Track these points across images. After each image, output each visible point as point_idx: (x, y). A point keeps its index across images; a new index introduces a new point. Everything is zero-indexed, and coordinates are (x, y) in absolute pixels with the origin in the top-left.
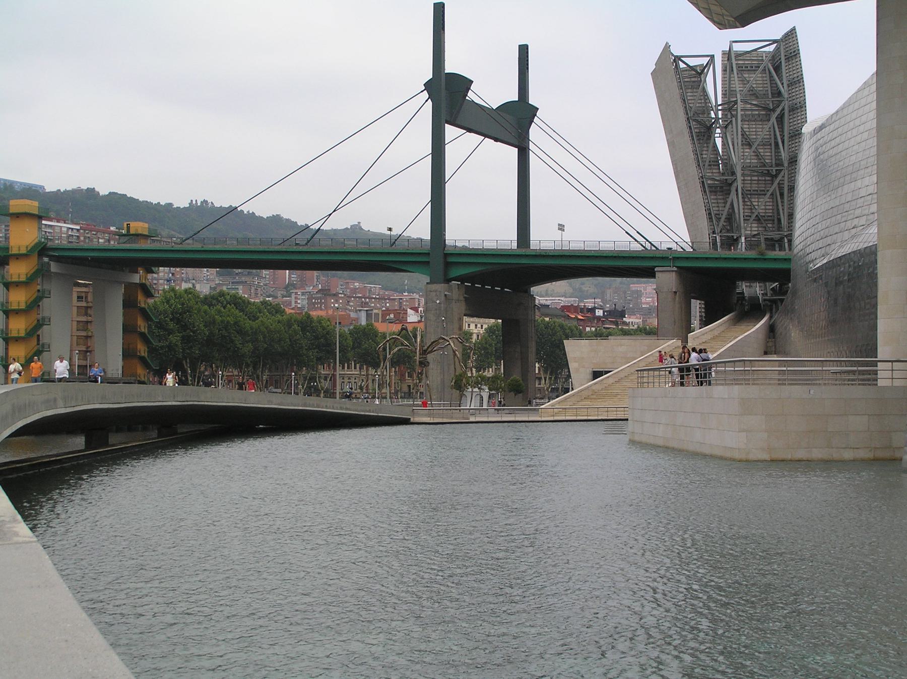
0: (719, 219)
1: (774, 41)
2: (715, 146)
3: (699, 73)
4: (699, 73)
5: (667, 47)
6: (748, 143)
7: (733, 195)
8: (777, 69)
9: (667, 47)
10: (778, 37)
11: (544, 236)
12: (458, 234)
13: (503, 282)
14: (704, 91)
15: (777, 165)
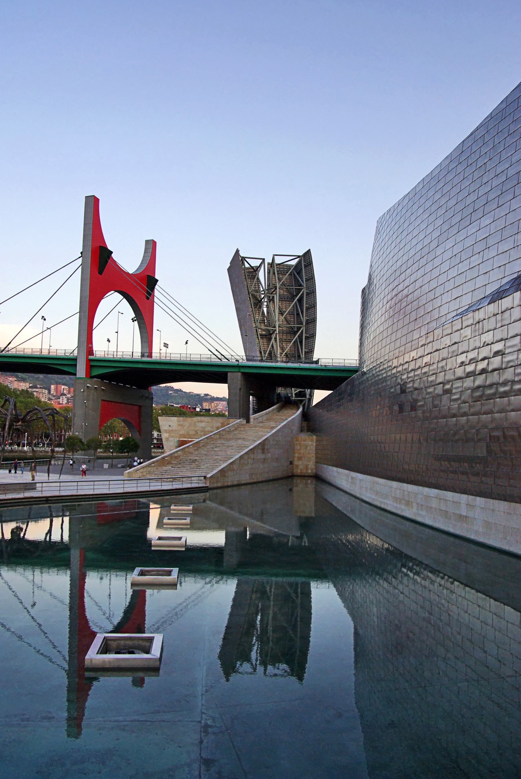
0: (265, 353)
1: (299, 257)
2: (263, 312)
3: (255, 270)
4: (255, 270)
5: (238, 251)
6: (281, 313)
7: (273, 340)
8: (299, 273)
9: (238, 251)
10: (301, 254)
11: (158, 352)
12: (101, 348)
13: (133, 384)
14: (258, 279)
15: (298, 324)
